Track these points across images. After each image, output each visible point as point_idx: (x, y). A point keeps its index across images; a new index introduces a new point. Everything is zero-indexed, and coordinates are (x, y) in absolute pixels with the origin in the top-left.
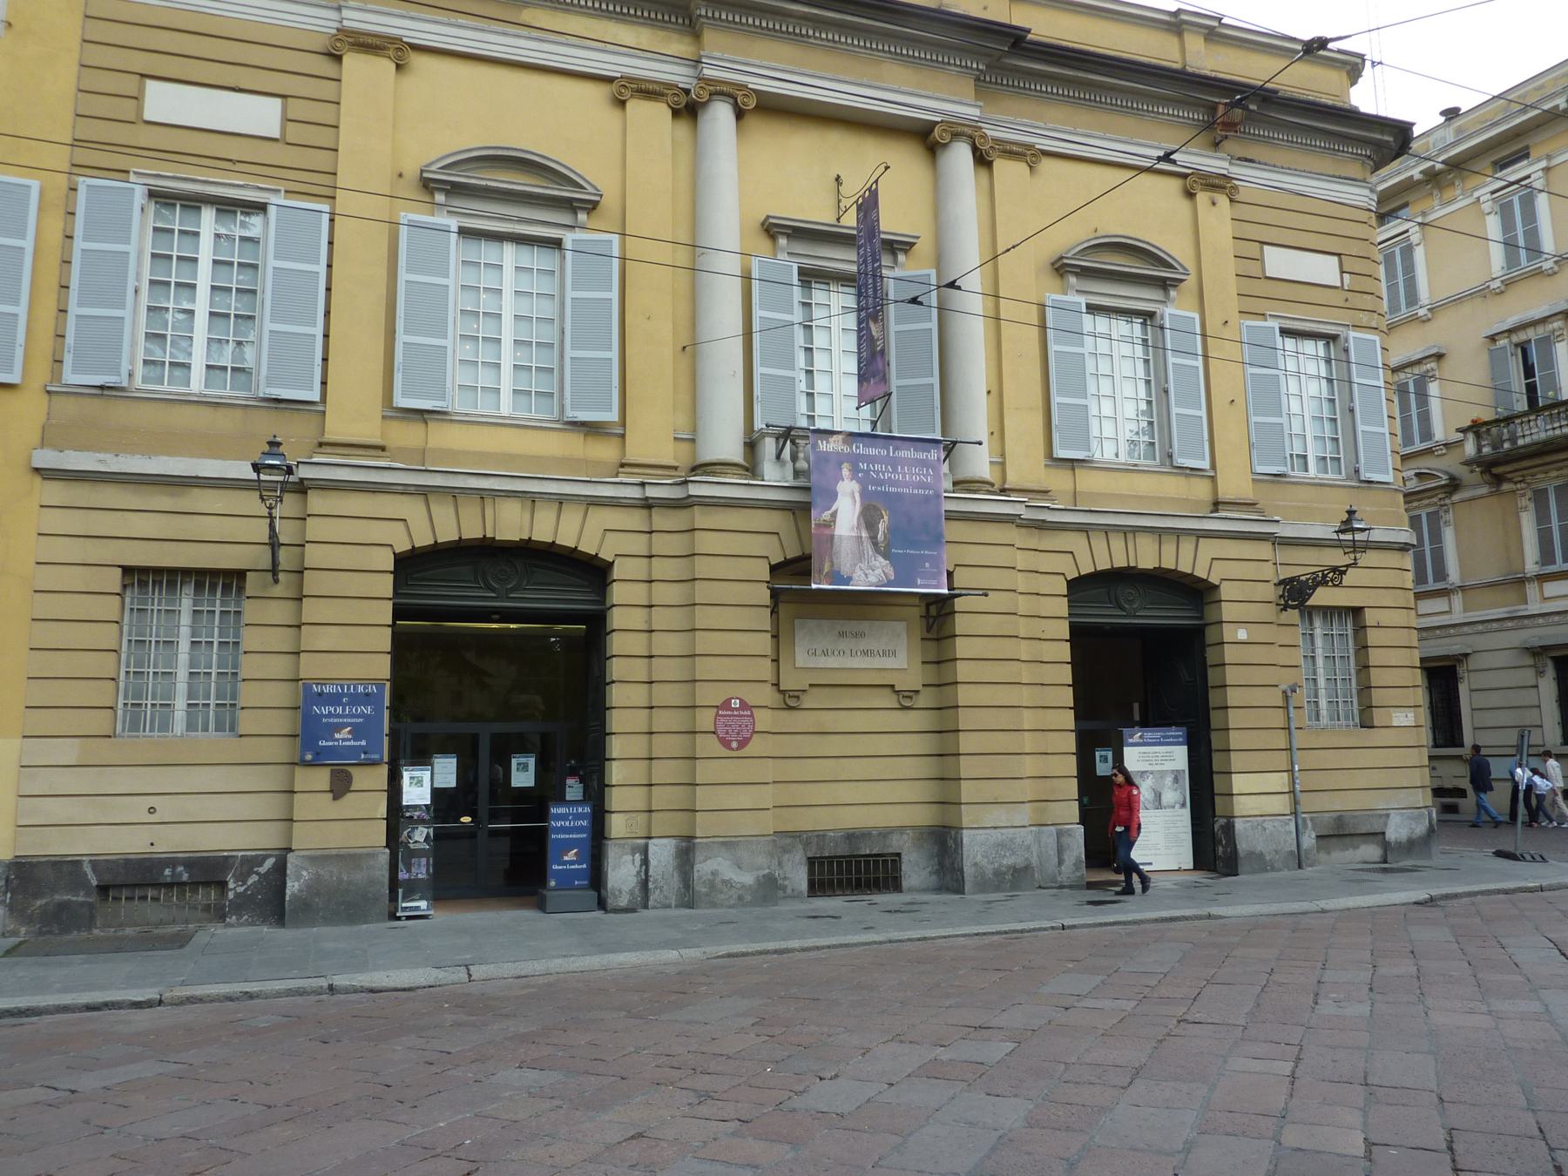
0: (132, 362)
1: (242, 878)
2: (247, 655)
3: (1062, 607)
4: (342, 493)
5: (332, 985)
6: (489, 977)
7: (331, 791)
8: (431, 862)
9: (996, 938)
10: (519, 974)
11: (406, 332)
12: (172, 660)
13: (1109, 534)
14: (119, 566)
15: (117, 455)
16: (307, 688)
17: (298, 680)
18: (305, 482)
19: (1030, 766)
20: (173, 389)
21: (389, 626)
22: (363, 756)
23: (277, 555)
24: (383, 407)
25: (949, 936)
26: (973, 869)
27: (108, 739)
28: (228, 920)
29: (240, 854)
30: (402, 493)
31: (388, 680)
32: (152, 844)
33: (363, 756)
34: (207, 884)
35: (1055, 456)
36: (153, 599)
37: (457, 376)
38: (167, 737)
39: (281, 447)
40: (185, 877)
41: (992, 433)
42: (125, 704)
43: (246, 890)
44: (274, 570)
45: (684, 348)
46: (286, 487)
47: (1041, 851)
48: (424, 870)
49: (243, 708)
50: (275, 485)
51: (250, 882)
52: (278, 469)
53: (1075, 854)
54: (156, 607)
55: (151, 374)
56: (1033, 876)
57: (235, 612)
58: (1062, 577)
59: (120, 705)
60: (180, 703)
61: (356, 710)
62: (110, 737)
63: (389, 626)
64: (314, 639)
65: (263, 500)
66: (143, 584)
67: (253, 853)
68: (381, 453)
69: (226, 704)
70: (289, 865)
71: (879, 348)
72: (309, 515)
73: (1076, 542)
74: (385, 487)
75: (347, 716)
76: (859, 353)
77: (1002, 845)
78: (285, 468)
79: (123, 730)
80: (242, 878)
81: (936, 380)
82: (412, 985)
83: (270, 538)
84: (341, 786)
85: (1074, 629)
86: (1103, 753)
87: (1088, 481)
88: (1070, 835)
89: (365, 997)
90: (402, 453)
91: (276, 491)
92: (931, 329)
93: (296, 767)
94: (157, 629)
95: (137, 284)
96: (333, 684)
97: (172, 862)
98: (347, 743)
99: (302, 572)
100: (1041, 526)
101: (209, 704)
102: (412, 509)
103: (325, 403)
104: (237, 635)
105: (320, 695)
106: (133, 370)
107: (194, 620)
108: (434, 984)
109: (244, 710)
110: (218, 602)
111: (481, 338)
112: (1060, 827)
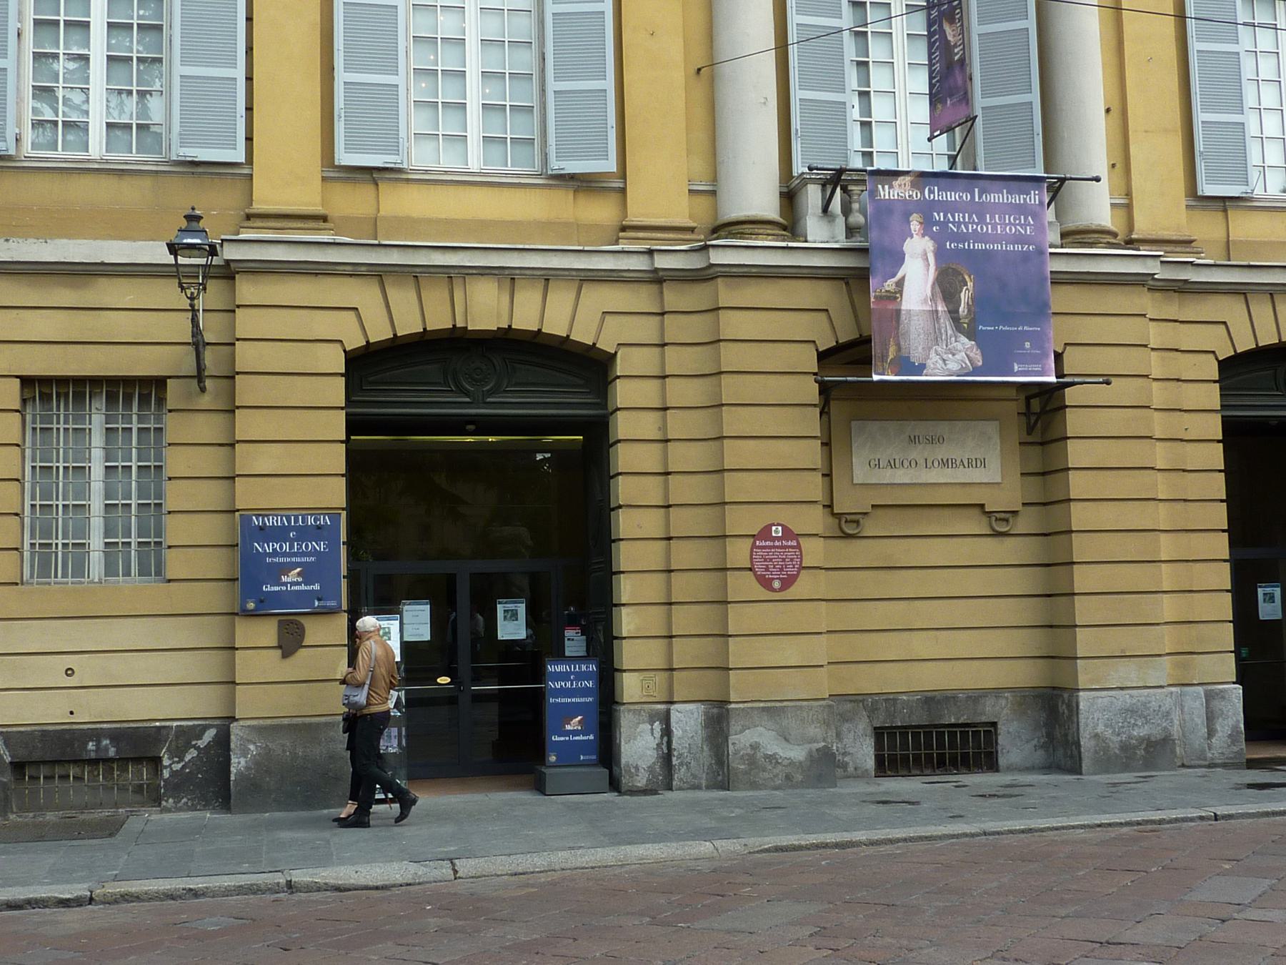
0: (19, 124)
1: (178, 753)
2: (172, 481)
3: (1211, 396)
4: (275, 277)
5: (291, 881)
6: (478, 874)
7: (280, 647)
8: (404, 733)
9: (1125, 830)
10: (516, 870)
11: (346, 69)
12: (83, 492)
13: (1275, 296)
14: (17, 377)
15: (7, 240)
16: (246, 520)
17: (234, 511)
18: (232, 265)
19: (1168, 608)
20: (70, 155)
21: (342, 442)
22: (317, 603)
23: (202, 358)
24: (322, 167)
25: (1063, 828)
26: (1093, 743)
27: (15, 587)
28: (164, 803)
29: (175, 724)
30: (351, 275)
31: (343, 509)
32: (72, 713)
33: (317, 603)
34: (137, 760)
35: (1200, 193)
36: (58, 416)
37: (412, 121)
38: (81, 583)
39: (202, 221)
40: (112, 752)
41: (1113, 166)
42: (31, 544)
43: (183, 767)
44: (200, 376)
45: (699, 70)
46: (209, 272)
47: (1184, 720)
48: (395, 743)
49: (170, 547)
50: (195, 269)
51: (188, 758)
52: (199, 249)
53: (1231, 722)
54: (62, 426)
55: (41, 140)
56: (1173, 751)
57: (155, 429)
58: (1211, 356)
59: (27, 546)
60: (96, 541)
61: (307, 546)
62: (17, 584)
63: (342, 442)
64: (250, 461)
65: (183, 289)
66: (45, 398)
67: (190, 723)
68: (322, 225)
69: (150, 543)
70: (232, 737)
71: (956, 58)
72: (238, 306)
73: (1232, 310)
74: (330, 267)
75: (295, 555)
76: (931, 65)
77: (1131, 711)
78: (207, 247)
79: (32, 576)
80: (178, 753)
81: (1035, 97)
82: (387, 883)
83: (193, 336)
84: (290, 641)
85: (1227, 424)
86: (1269, 590)
87: (1245, 227)
88: (1223, 698)
89: (330, 897)
90: (347, 223)
91: (198, 277)
92: (1028, 29)
93: (237, 618)
94: (64, 452)
95: (19, 25)
96: (277, 516)
97: (96, 735)
98: (296, 588)
99: (233, 378)
100: (1183, 289)
101: (130, 543)
102: (365, 295)
103: (252, 165)
104: (159, 457)
105: (261, 528)
106: (20, 133)
107: (107, 441)
108: (412, 881)
109: (172, 550)
110: (135, 418)
111: (440, 72)
112: (1210, 687)
